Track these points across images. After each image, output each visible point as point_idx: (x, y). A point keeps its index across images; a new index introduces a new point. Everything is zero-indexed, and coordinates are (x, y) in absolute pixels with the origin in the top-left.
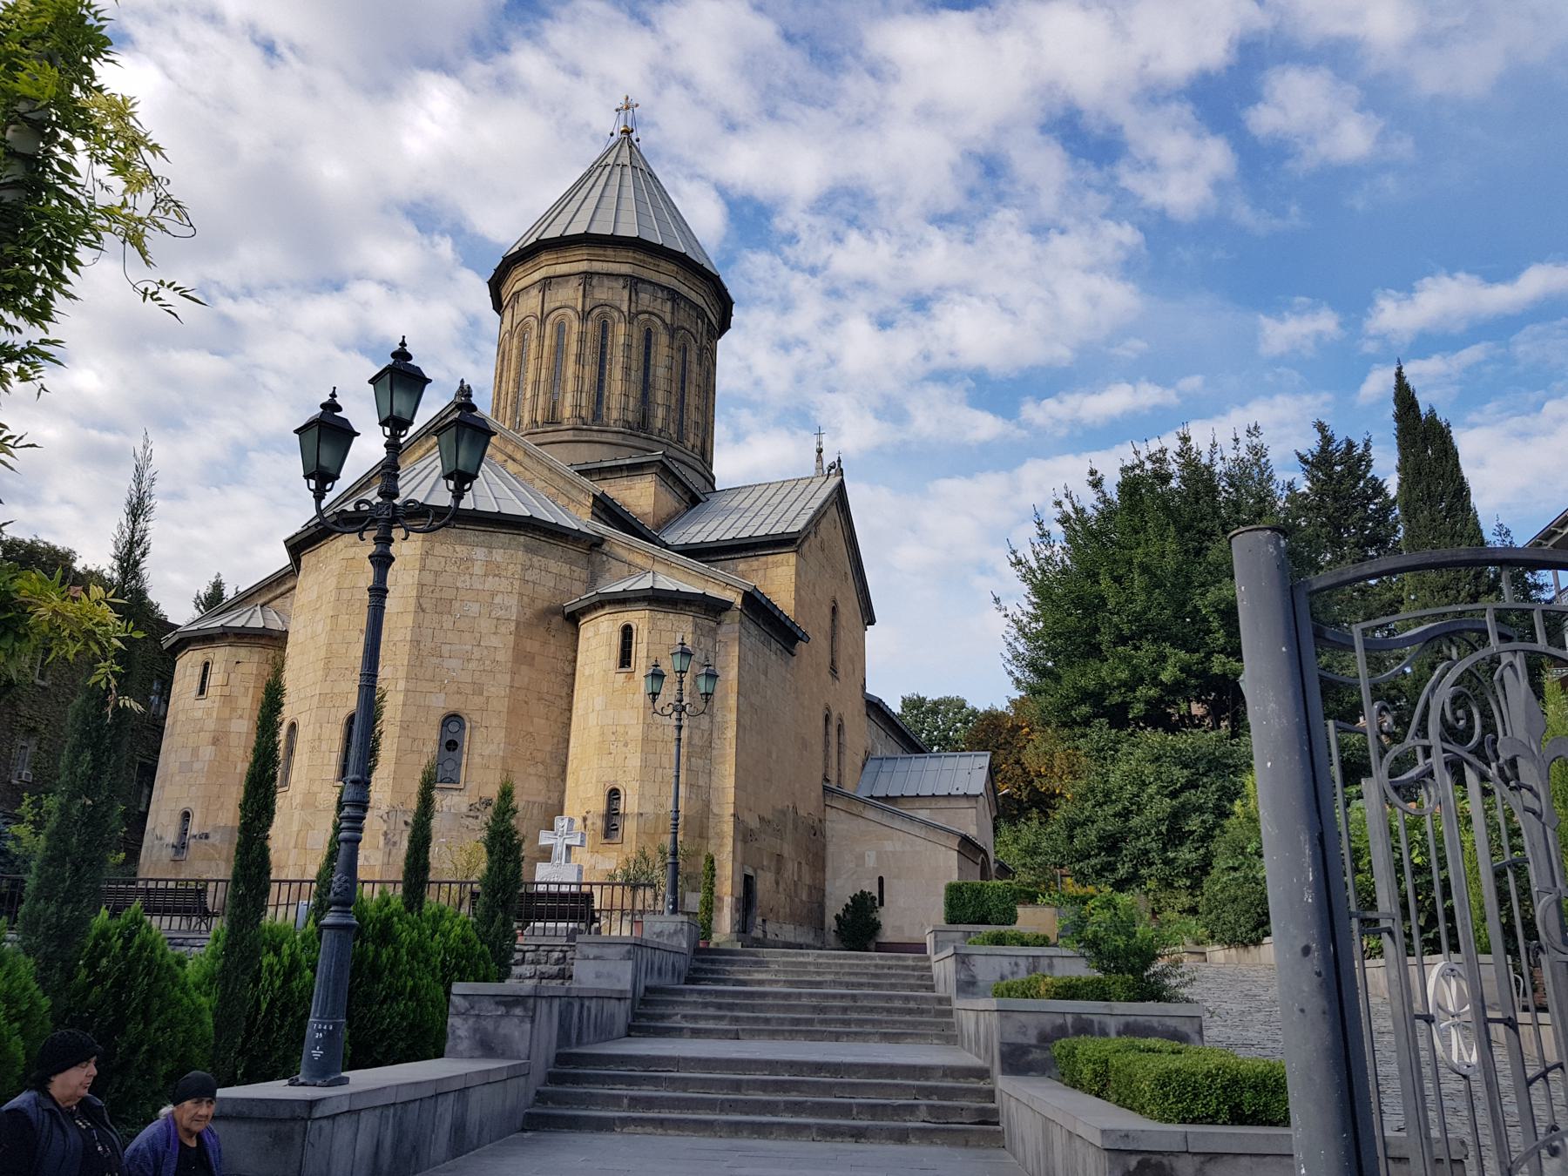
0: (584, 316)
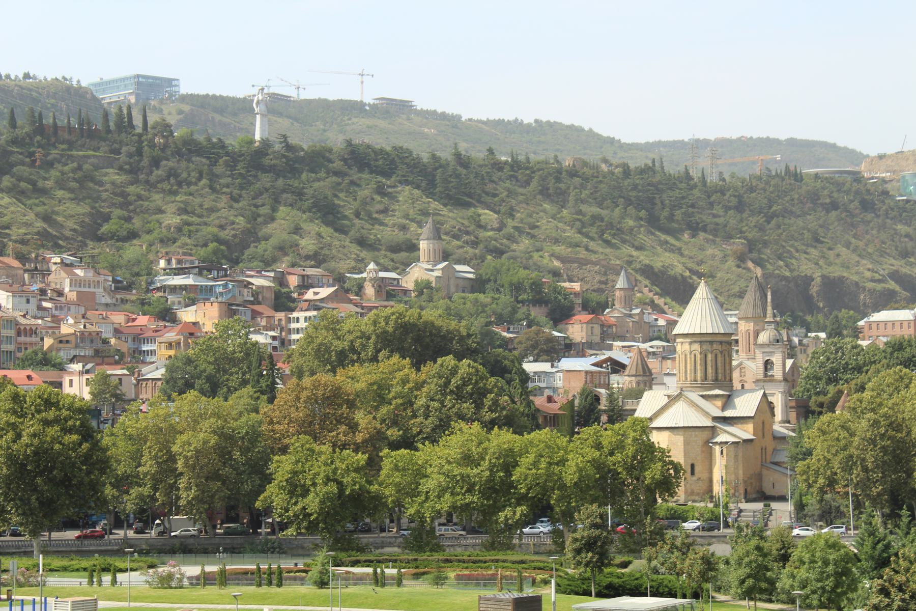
0: (701, 353)
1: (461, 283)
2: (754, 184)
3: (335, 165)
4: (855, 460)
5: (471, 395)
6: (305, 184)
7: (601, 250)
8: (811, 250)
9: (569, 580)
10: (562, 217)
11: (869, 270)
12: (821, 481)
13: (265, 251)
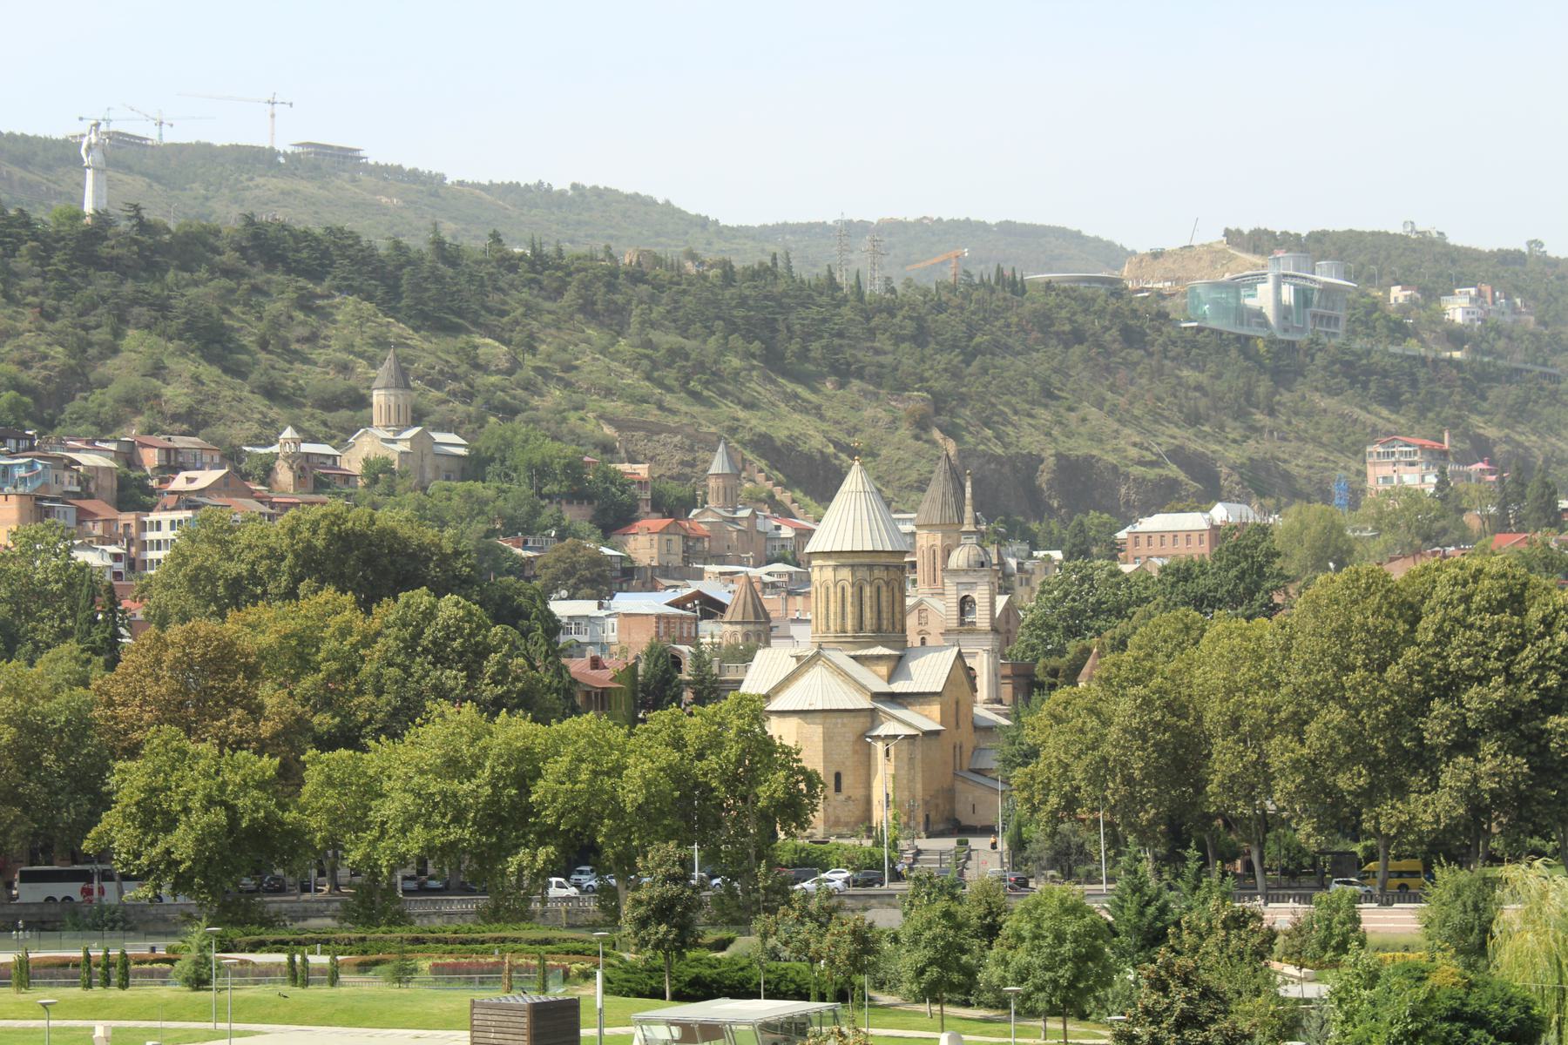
0: (853, 585)
1: (444, 463)
2: (944, 299)
3: (224, 258)
4: (1111, 764)
5: (461, 655)
6: (172, 290)
7: (684, 408)
8: (1039, 411)
9: (626, 972)
10: (618, 352)
11: (1135, 445)
12: (1053, 800)
13: (102, 405)
